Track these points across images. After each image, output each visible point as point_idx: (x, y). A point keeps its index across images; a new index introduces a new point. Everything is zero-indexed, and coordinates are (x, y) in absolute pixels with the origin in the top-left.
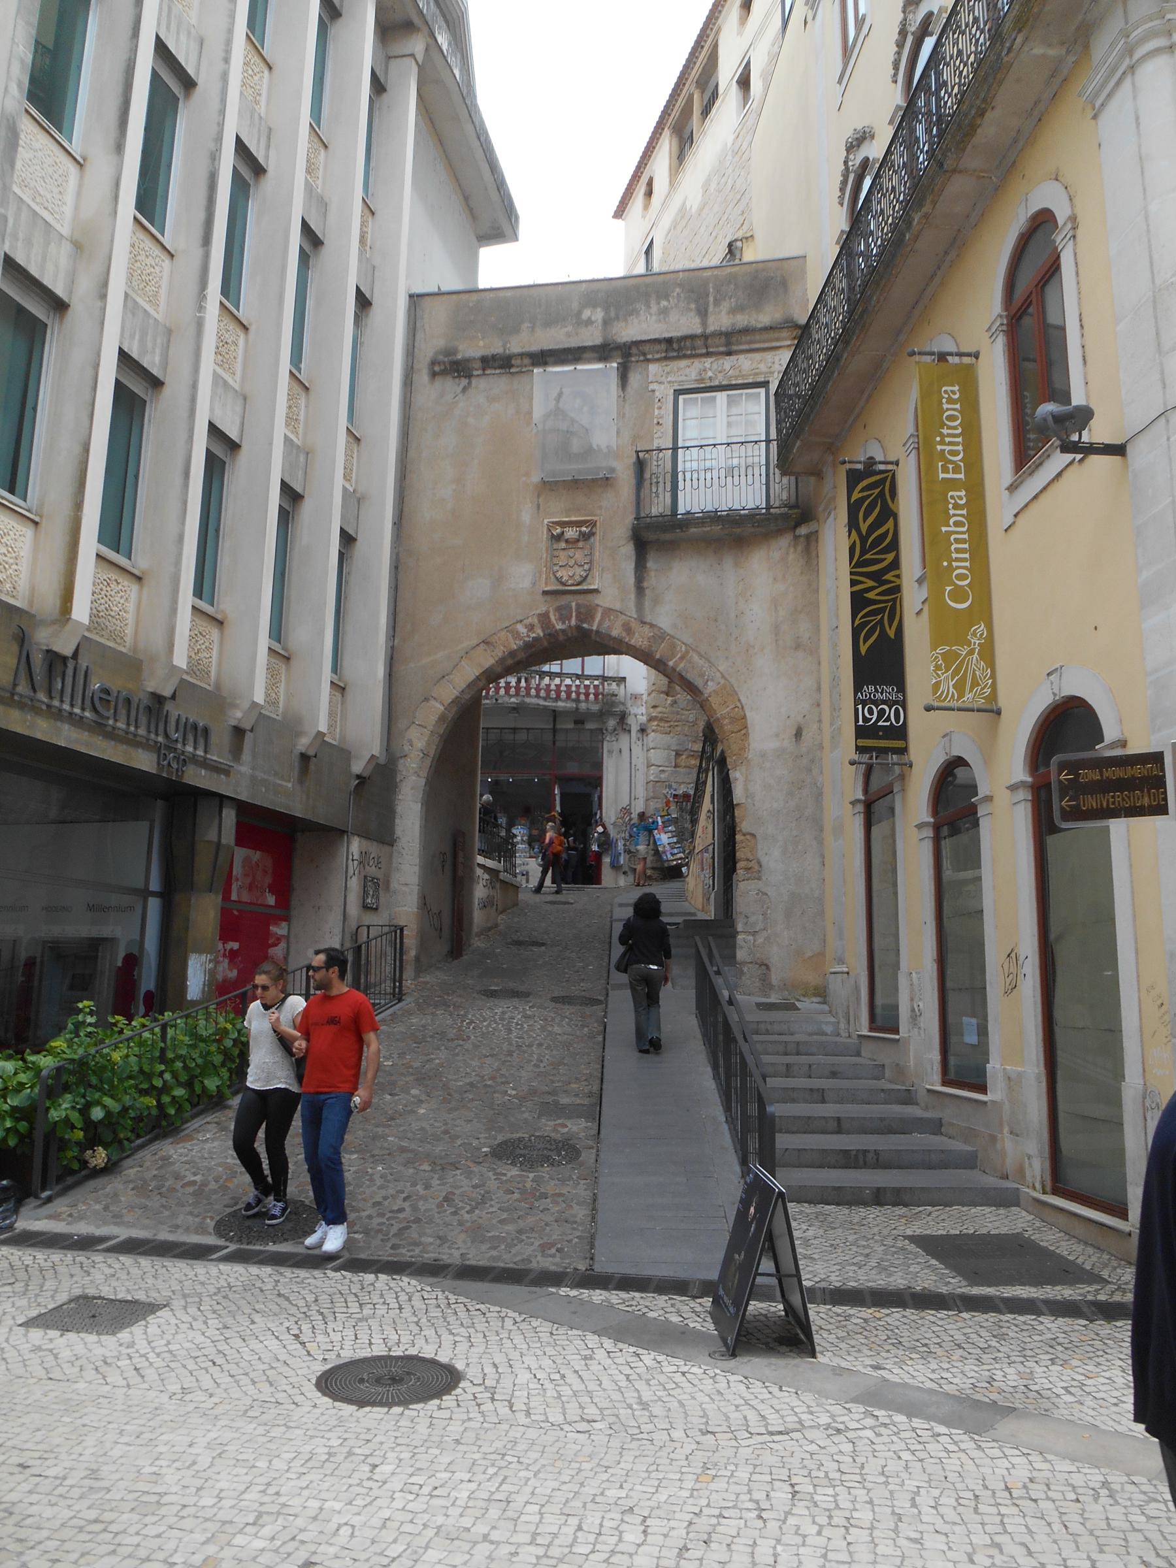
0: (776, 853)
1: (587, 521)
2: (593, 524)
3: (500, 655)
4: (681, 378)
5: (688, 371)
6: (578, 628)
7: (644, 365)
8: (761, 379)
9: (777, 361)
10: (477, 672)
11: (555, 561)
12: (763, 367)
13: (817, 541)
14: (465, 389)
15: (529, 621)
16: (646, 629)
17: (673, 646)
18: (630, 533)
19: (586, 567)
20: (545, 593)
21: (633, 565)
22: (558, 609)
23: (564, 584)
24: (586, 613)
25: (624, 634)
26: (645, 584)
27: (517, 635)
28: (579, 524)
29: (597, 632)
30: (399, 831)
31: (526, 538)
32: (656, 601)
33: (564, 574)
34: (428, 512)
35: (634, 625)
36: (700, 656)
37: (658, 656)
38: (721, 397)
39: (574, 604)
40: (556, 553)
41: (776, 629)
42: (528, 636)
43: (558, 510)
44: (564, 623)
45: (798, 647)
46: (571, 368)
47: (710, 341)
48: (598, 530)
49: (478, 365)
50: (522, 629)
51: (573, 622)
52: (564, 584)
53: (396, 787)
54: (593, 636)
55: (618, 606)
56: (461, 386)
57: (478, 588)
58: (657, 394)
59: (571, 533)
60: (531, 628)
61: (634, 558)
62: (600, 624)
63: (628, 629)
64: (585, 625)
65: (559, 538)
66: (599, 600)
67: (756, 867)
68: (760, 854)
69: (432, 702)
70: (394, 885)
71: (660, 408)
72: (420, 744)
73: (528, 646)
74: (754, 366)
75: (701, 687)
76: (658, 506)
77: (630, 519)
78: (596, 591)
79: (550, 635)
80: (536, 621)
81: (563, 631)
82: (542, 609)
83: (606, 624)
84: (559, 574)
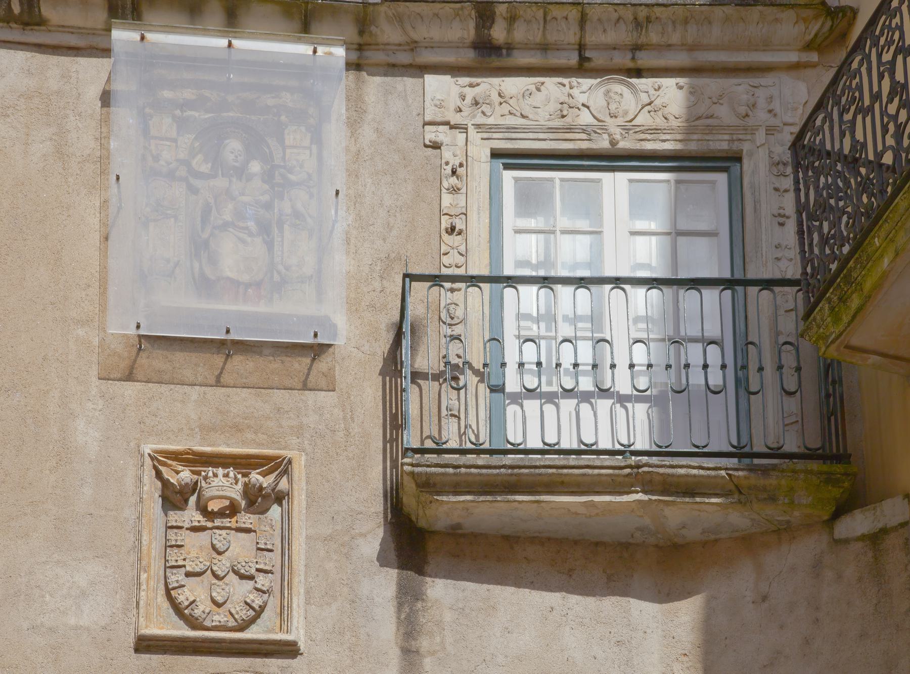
1: (268, 459)
2: (279, 466)
4: (510, 121)
8: (720, 144)
9: (762, 103)
11: (174, 557)
12: (724, 113)
20: (146, 645)
26: (424, 643)
28: (243, 463)
33: (193, 592)
48: (299, 486)
52: (193, 623)
58: (447, 154)
59: (223, 485)
71: (455, 190)
78: (289, 650)
84: (183, 597)
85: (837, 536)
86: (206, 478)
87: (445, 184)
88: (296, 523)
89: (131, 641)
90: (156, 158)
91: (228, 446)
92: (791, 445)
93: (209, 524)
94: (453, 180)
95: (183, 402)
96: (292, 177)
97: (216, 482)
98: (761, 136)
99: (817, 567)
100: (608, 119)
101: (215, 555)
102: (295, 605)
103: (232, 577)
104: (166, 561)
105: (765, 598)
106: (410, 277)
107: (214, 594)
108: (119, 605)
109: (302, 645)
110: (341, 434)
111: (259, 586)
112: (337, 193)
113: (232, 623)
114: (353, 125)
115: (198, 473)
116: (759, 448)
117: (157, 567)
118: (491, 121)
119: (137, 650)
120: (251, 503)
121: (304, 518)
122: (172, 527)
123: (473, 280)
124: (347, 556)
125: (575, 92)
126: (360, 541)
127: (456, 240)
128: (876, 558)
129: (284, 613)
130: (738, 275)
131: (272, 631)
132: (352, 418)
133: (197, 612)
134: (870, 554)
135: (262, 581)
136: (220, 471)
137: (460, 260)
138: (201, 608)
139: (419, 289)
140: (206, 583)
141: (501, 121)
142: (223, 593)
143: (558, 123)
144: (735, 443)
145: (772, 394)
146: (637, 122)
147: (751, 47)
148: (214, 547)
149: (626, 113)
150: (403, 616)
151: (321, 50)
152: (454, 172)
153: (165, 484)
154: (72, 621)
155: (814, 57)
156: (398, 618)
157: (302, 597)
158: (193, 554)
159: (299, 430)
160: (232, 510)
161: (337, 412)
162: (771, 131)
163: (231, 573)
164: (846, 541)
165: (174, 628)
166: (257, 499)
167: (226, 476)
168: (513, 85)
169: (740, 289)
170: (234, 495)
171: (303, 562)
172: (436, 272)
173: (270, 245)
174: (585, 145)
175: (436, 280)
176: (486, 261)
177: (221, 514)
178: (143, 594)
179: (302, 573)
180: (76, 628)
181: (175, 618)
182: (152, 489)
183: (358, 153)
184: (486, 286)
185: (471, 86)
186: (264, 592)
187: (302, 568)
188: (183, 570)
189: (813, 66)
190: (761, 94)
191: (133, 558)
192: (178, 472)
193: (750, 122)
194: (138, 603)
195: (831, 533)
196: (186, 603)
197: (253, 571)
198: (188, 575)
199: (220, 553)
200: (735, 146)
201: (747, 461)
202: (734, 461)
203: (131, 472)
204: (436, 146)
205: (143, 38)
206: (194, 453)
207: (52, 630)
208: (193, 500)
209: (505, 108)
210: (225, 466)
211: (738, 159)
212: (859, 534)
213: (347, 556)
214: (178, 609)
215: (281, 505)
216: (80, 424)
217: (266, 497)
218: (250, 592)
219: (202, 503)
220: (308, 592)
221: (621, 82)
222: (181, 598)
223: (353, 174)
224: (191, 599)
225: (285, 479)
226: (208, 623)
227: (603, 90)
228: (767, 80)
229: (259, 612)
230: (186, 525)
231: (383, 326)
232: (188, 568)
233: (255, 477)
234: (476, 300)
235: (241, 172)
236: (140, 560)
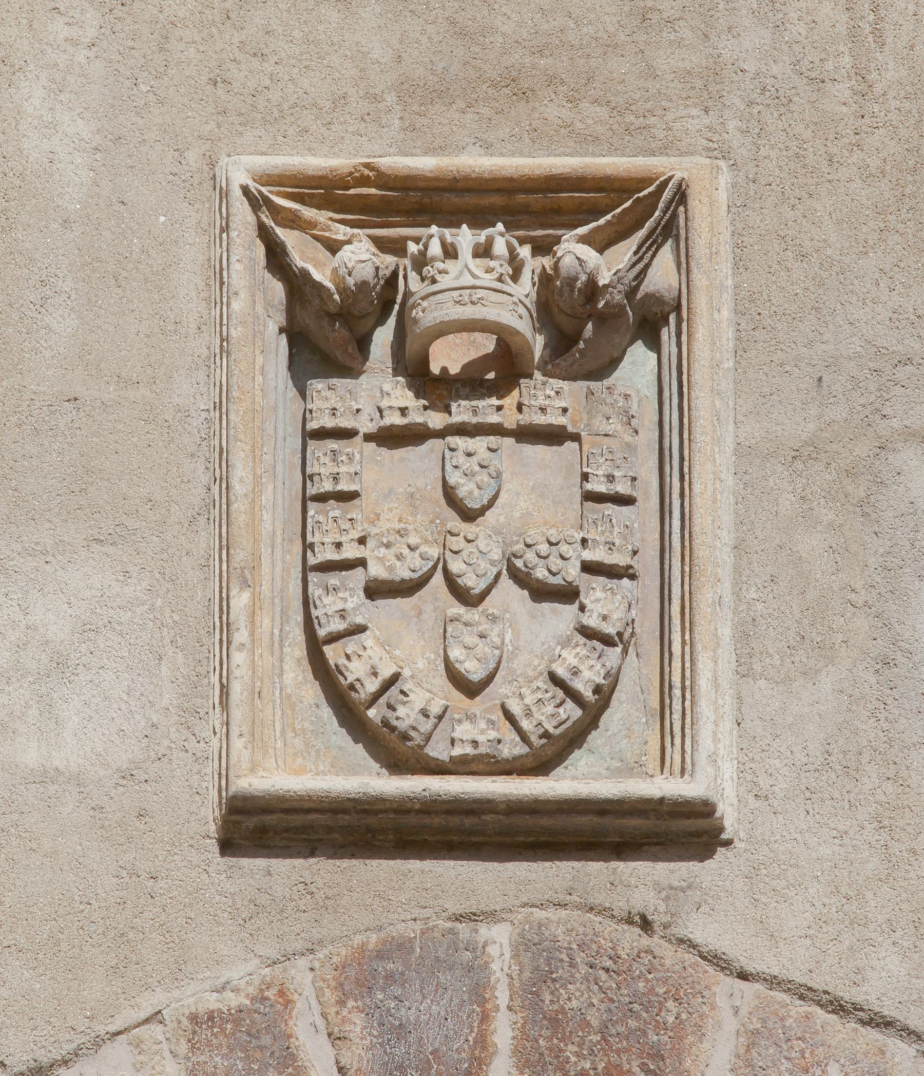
1: (614, 188)
2: (647, 210)
11: (331, 532)
20: (256, 827)
28: (532, 207)
33: (394, 649)
39: (498, 939)
48: (712, 275)
52: (394, 750)
59: (475, 286)
78: (685, 831)
82: (231, 975)
84: (360, 666)
86: (421, 262)
88: (703, 402)
91: (488, 148)
93: (436, 420)
97: (452, 274)
101: (455, 522)
102: (704, 683)
103: (509, 594)
104: (307, 547)
107: (455, 653)
108: (168, 698)
109: (729, 815)
110: (842, 90)
111: (592, 621)
113: (512, 748)
115: (396, 247)
117: (279, 569)
119: (227, 846)
120: (562, 342)
121: (727, 385)
122: (322, 434)
124: (866, 509)
129: (671, 708)
131: (634, 769)
132: (877, 33)
133: (406, 716)
135: (603, 603)
136: (465, 238)
138: (418, 699)
140: (430, 617)
142: (483, 648)
148: (450, 496)
153: (298, 286)
154: (31, 755)
158: (388, 523)
160: (504, 368)
163: (506, 582)
165: (337, 768)
166: (584, 330)
167: (483, 251)
171: (727, 537)
177: (471, 383)
178: (239, 658)
179: (726, 574)
180: (45, 777)
181: (339, 737)
182: (258, 305)
186: (607, 641)
187: (726, 556)
188: (357, 577)
191: (205, 540)
192: (333, 247)
194: (225, 690)
196: (372, 686)
197: (573, 572)
199: (469, 516)
203: (194, 252)
206: (383, 180)
208: (383, 338)
210: (479, 218)
213: (866, 509)
215: (654, 344)
217: (607, 319)
218: (566, 643)
219: (412, 347)
220: (743, 635)
222: (355, 670)
224: (386, 672)
225: (666, 254)
226: (438, 751)
229: (594, 708)
230: (366, 425)
232: (376, 570)
233: (574, 251)
236: (226, 546)
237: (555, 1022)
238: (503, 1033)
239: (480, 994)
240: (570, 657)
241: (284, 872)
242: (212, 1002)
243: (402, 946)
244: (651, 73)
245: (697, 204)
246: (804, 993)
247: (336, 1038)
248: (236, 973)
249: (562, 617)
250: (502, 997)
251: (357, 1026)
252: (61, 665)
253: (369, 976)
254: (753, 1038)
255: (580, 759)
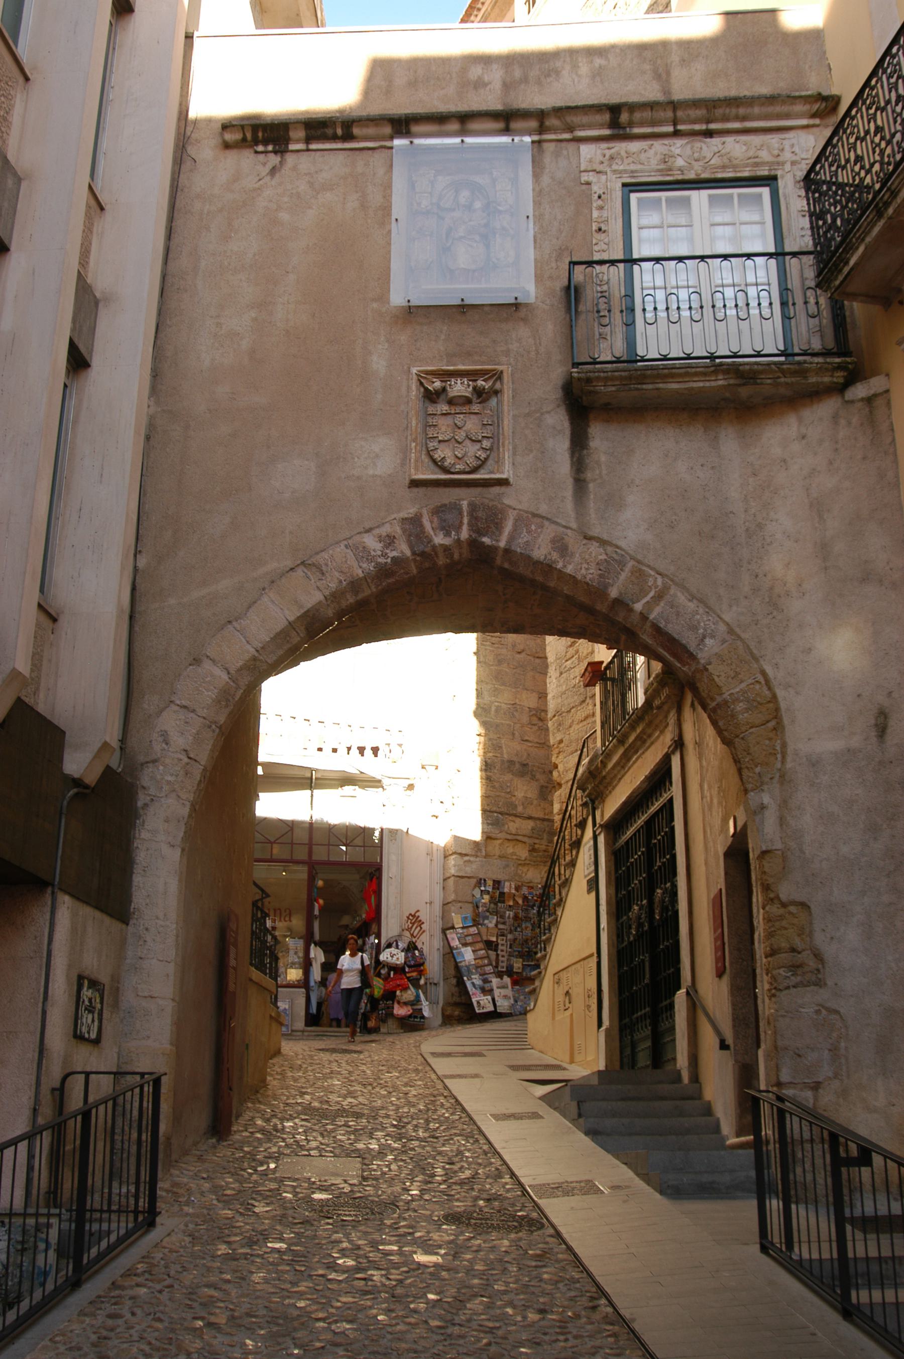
0: (852, 935)
3: (333, 585)
4: (633, 167)
5: (645, 156)
6: (473, 543)
7: (572, 146)
8: (764, 172)
9: (787, 148)
10: (292, 614)
11: (431, 432)
12: (765, 155)
13: (888, 404)
14: (273, 171)
15: (385, 530)
16: (594, 549)
17: (639, 574)
18: (559, 394)
19: (486, 444)
20: (415, 484)
21: (566, 444)
22: (438, 511)
23: (446, 471)
24: (488, 519)
25: (555, 556)
26: (589, 475)
27: (363, 553)
28: (472, 375)
29: (507, 551)
30: (138, 899)
31: (379, 396)
32: (613, 501)
33: (444, 453)
34: (206, 351)
35: (571, 539)
36: (692, 598)
37: (614, 593)
38: (699, 198)
39: (465, 504)
40: (430, 420)
41: (824, 549)
42: (384, 555)
43: (434, 351)
44: (448, 534)
45: (865, 579)
46: (457, 140)
47: (680, 114)
49: (301, 134)
50: (372, 543)
51: (465, 534)
53: (137, 816)
54: (498, 561)
55: (543, 509)
56: (269, 166)
57: (294, 475)
58: (595, 188)
60: (389, 541)
61: (568, 432)
62: (512, 538)
63: (562, 548)
64: (486, 540)
65: (431, 397)
66: (509, 498)
67: (812, 963)
68: (820, 939)
69: (207, 665)
70: (128, 998)
71: (601, 208)
72: (179, 741)
73: (383, 572)
74: (751, 154)
75: (692, 647)
76: (610, 348)
77: (558, 373)
78: (504, 482)
79: (423, 554)
80: (398, 530)
81: (446, 549)
82: (410, 511)
83: (524, 537)
84: (438, 455)
85: (847, 398)
87: (595, 205)
89: (407, 482)
90: (419, 204)
91: (464, 365)
92: (817, 345)
94: (600, 202)
95: (436, 341)
96: (500, 208)
98: (788, 167)
99: (835, 418)
100: (693, 162)
103: (468, 442)
105: (803, 437)
106: (573, 263)
108: (399, 461)
109: (511, 480)
112: (528, 217)
114: (537, 176)
116: (796, 350)
118: (621, 168)
123: (613, 262)
125: (673, 149)
126: (547, 416)
127: (602, 236)
128: (871, 412)
129: (499, 462)
130: (779, 251)
131: (492, 472)
132: (540, 344)
133: (446, 464)
134: (867, 409)
137: (605, 247)
138: (449, 461)
139: (579, 269)
141: (627, 168)
143: (662, 166)
144: (782, 348)
145: (802, 317)
146: (712, 162)
147: (779, 117)
149: (705, 157)
150: (575, 459)
151: (517, 139)
152: (599, 197)
153: (426, 389)
154: (371, 472)
155: (817, 121)
156: (572, 460)
157: (511, 452)
159: (507, 353)
161: (531, 341)
162: (793, 163)
164: (852, 402)
165: (433, 473)
168: (634, 146)
169: (780, 258)
170: (467, 395)
172: (590, 259)
173: (487, 246)
174: (680, 177)
175: (590, 263)
176: (622, 252)
180: (374, 476)
183: (541, 191)
184: (621, 266)
185: (609, 149)
188: (437, 440)
189: (818, 126)
190: (787, 144)
193: (781, 159)
195: (843, 397)
197: (480, 438)
198: (440, 441)
200: (773, 173)
201: (790, 358)
202: (782, 359)
204: (588, 184)
205: (411, 142)
206: (443, 370)
207: (359, 478)
209: (631, 160)
211: (774, 178)
212: (860, 397)
214: (434, 461)
216: (375, 358)
221: (700, 141)
222: (436, 456)
223: (537, 203)
226: (452, 470)
227: (689, 146)
228: (791, 134)
231: (558, 289)
232: (440, 438)
234: (616, 274)
235: (469, 208)
237: (476, 518)
238: (465, 520)
239: (461, 513)
240: (479, 453)
241: (421, 491)
242: (406, 516)
243: (445, 505)
244: (495, 351)
245: (505, 374)
246: (527, 512)
247: (432, 522)
248: (411, 511)
249: (478, 446)
250: (465, 514)
251: (436, 520)
252: (377, 456)
253: (438, 511)
254: (516, 520)
255: (482, 471)
